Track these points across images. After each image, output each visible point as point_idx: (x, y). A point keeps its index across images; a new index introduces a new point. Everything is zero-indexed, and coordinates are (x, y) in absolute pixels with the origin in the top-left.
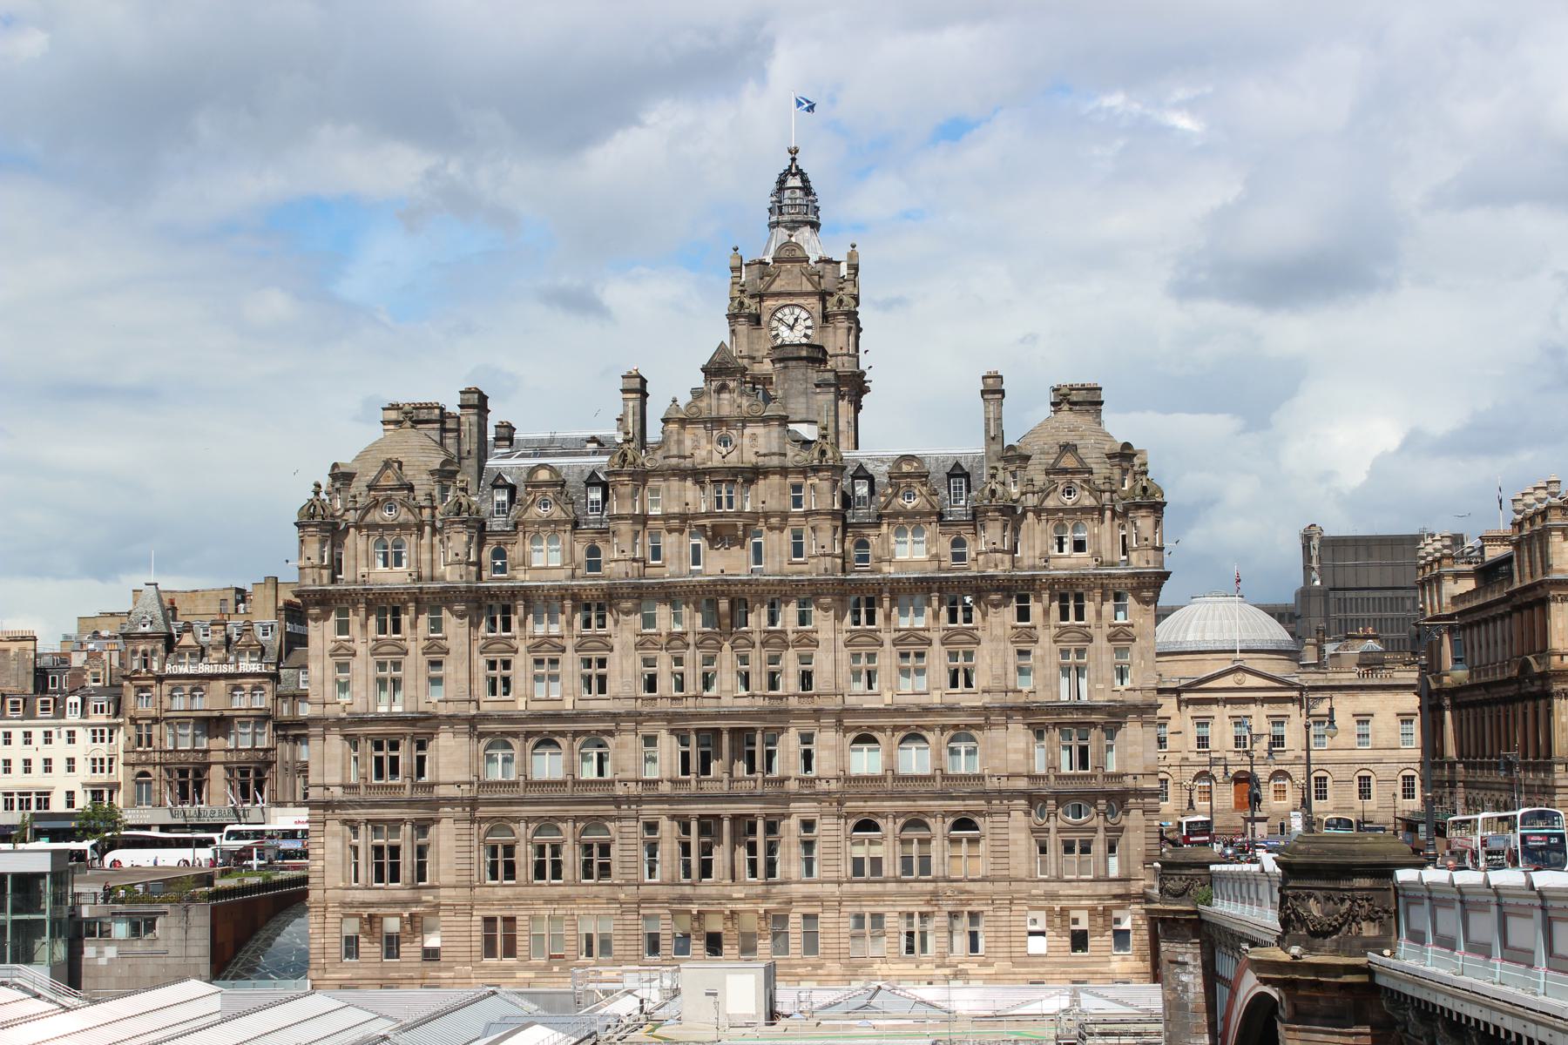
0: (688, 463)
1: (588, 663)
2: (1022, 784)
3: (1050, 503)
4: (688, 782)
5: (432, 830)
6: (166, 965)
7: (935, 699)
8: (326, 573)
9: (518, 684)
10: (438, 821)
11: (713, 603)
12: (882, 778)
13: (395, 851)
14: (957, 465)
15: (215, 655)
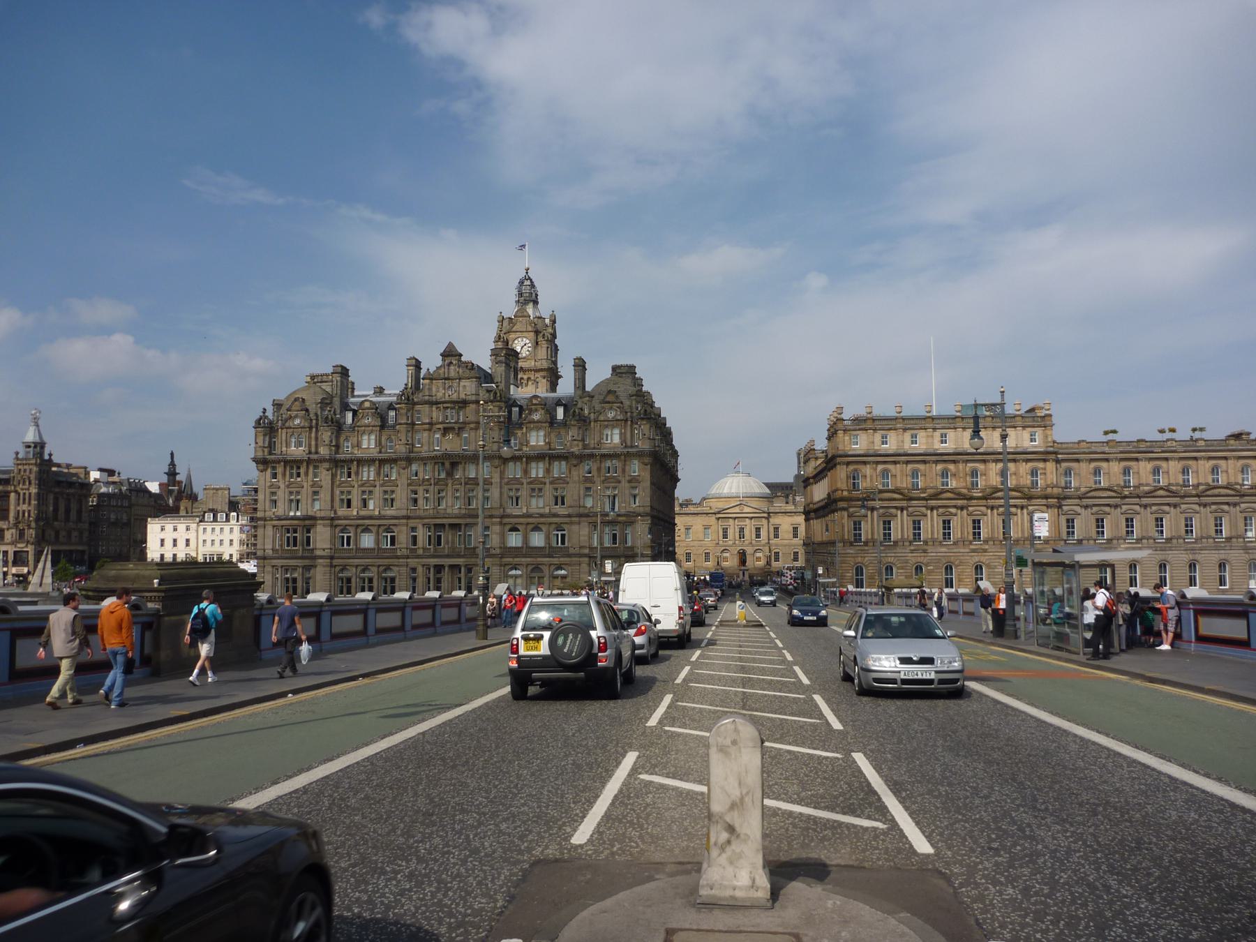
0: (434, 399)
2: (586, 551)
3: (602, 418)
11: (443, 464)
13: (295, 580)
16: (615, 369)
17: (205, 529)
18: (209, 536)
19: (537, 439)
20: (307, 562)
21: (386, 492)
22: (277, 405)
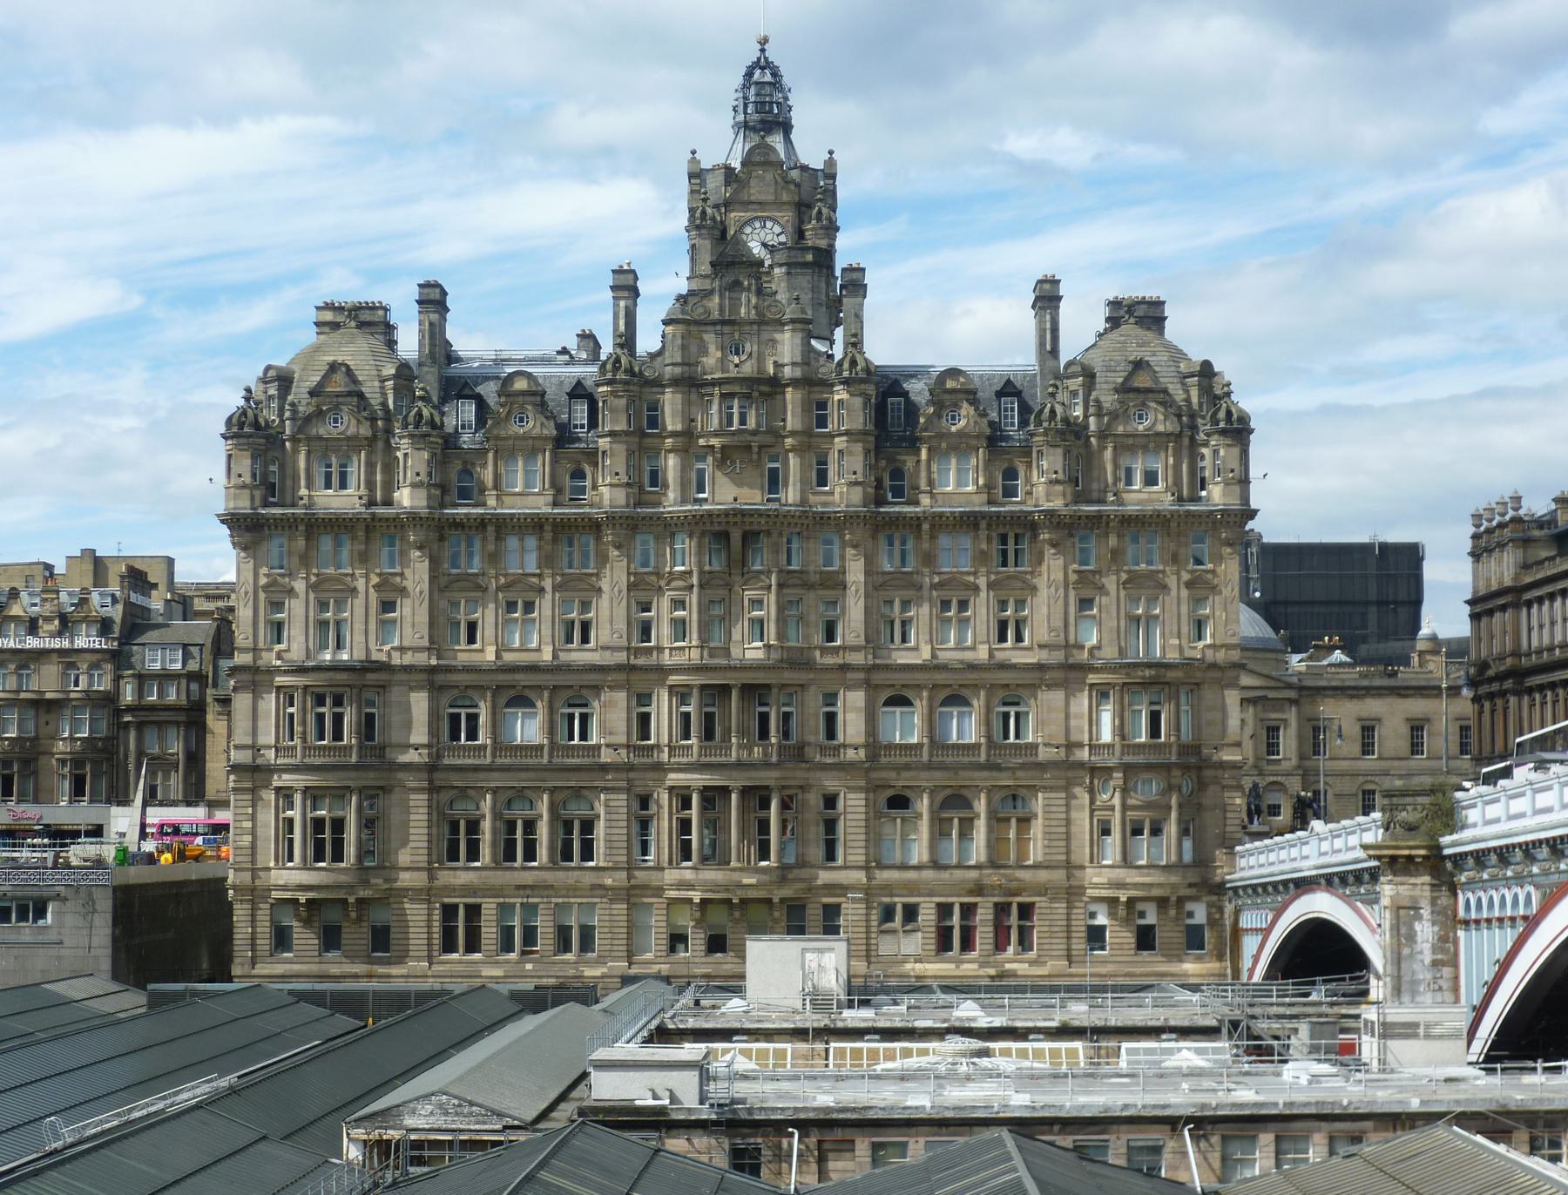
2: (1084, 755)
4: (690, 747)
5: (380, 802)
6: (59, 958)
7: (982, 654)
8: (257, 493)
9: (486, 631)
13: (338, 825)
14: (1009, 382)
15: (47, 627)
20: (370, 778)
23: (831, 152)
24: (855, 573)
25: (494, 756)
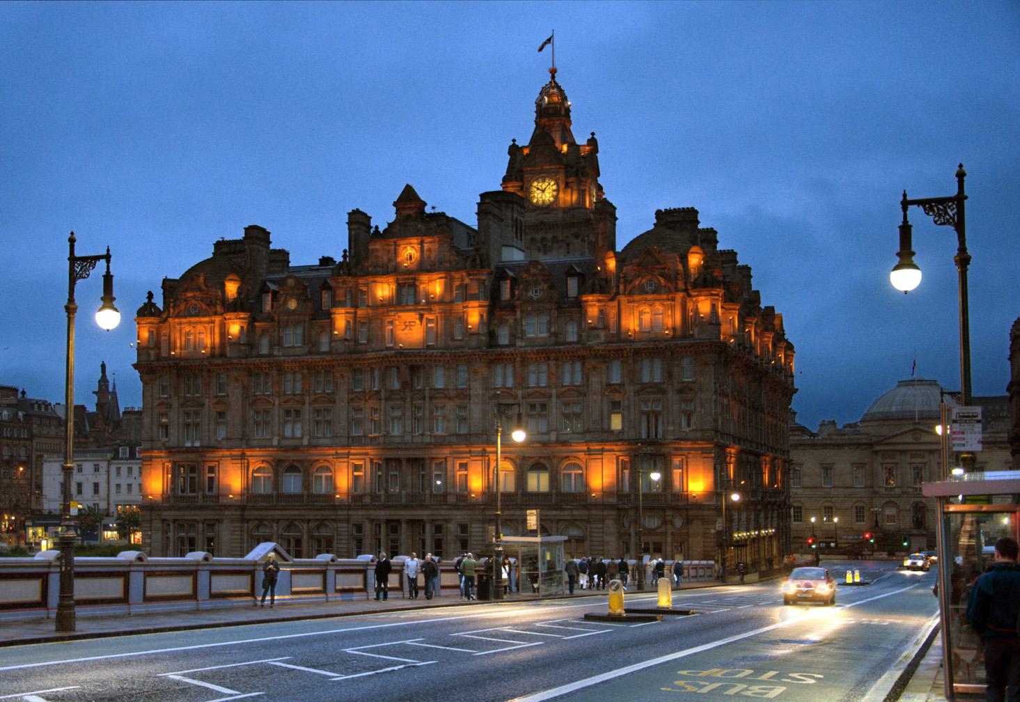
1: (318, 411)
2: (613, 500)
10: (219, 521)
12: (515, 494)
16: (659, 214)
17: (119, 469)
18: (124, 480)
19: (536, 329)
20: (209, 515)
21: (318, 411)
22: (168, 285)
23: (593, 134)
24: (477, 388)
25: (277, 501)
